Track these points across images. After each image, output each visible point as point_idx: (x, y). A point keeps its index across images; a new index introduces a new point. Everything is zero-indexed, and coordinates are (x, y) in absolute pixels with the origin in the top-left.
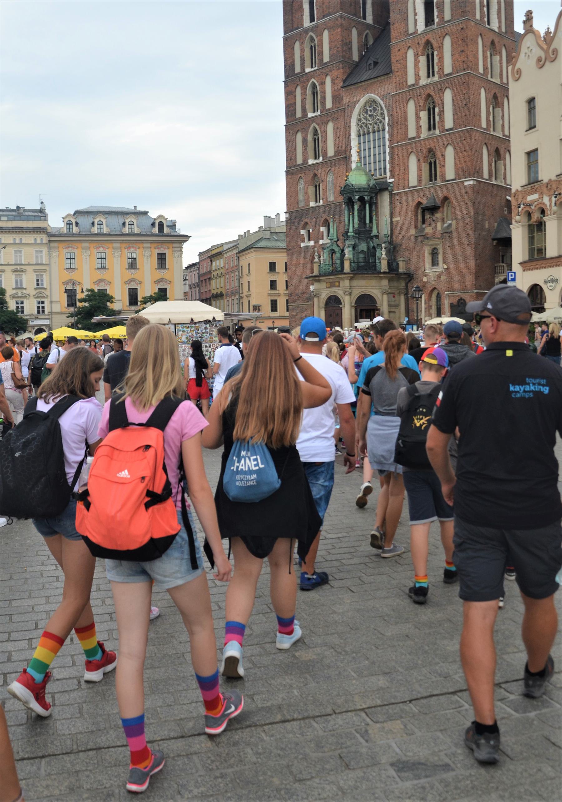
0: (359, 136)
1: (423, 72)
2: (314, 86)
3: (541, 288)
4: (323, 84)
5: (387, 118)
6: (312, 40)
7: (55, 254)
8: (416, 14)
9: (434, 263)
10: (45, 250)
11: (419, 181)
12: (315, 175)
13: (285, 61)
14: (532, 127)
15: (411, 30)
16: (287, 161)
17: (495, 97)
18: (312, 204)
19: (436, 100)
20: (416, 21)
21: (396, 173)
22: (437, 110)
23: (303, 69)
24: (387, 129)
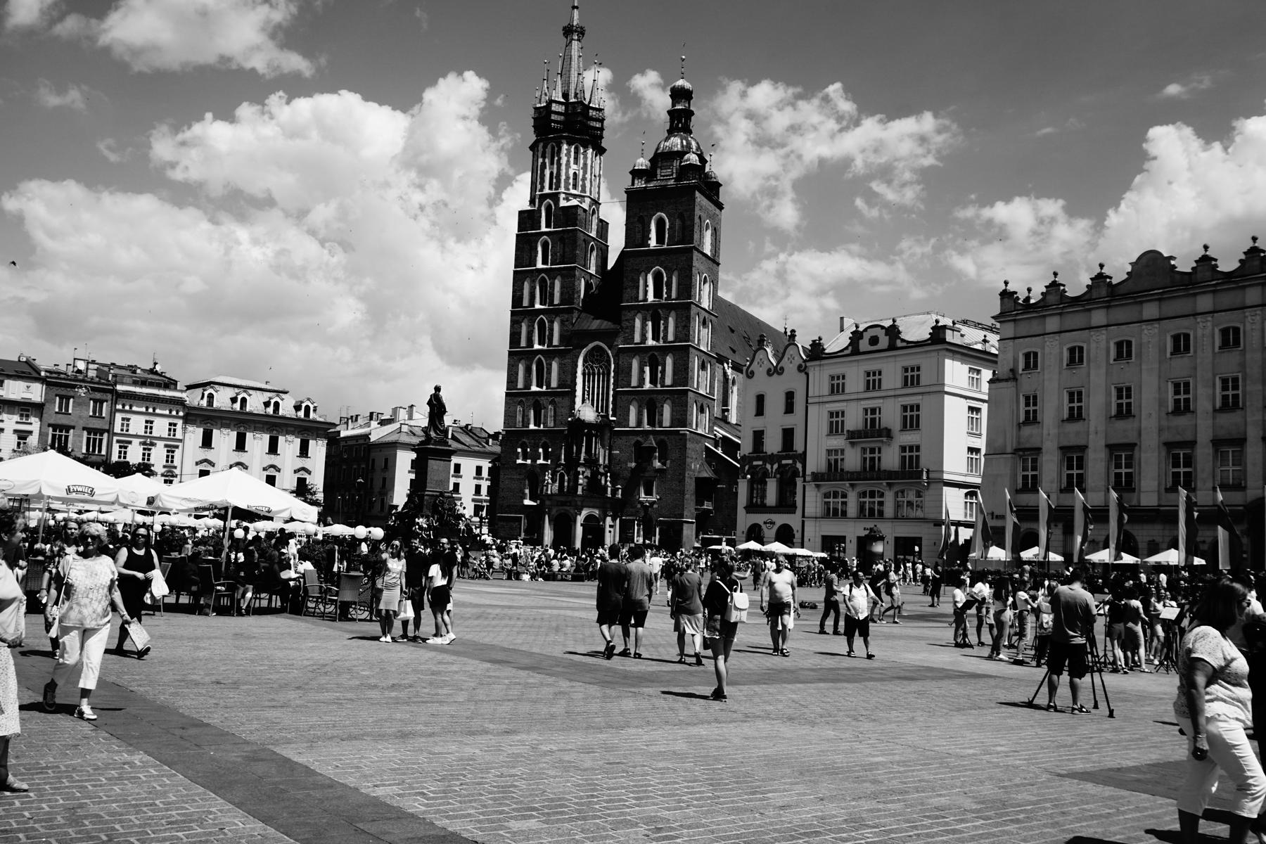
0: (584, 374)
1: (650, 335)
2: (542, 323)
3: (760, 526)
4: (551, 322)
5: (613, 366)
6: (543, 280)
7: (190, 428)
8: (646, 286)
9: (649, 492)
10: (180, 423)
11: (639, 423)
12: (537, 401)
13: (514, 292)
14: (760, 411)
15: (641, 297)
16: (508, 382)
17: (703, 362)
18: (532, 427)
19: (660, 359)
20: (646, 292)
21: (618, 415)
22: (660, 368)
23: (532, 303)
24: (612, 374)
